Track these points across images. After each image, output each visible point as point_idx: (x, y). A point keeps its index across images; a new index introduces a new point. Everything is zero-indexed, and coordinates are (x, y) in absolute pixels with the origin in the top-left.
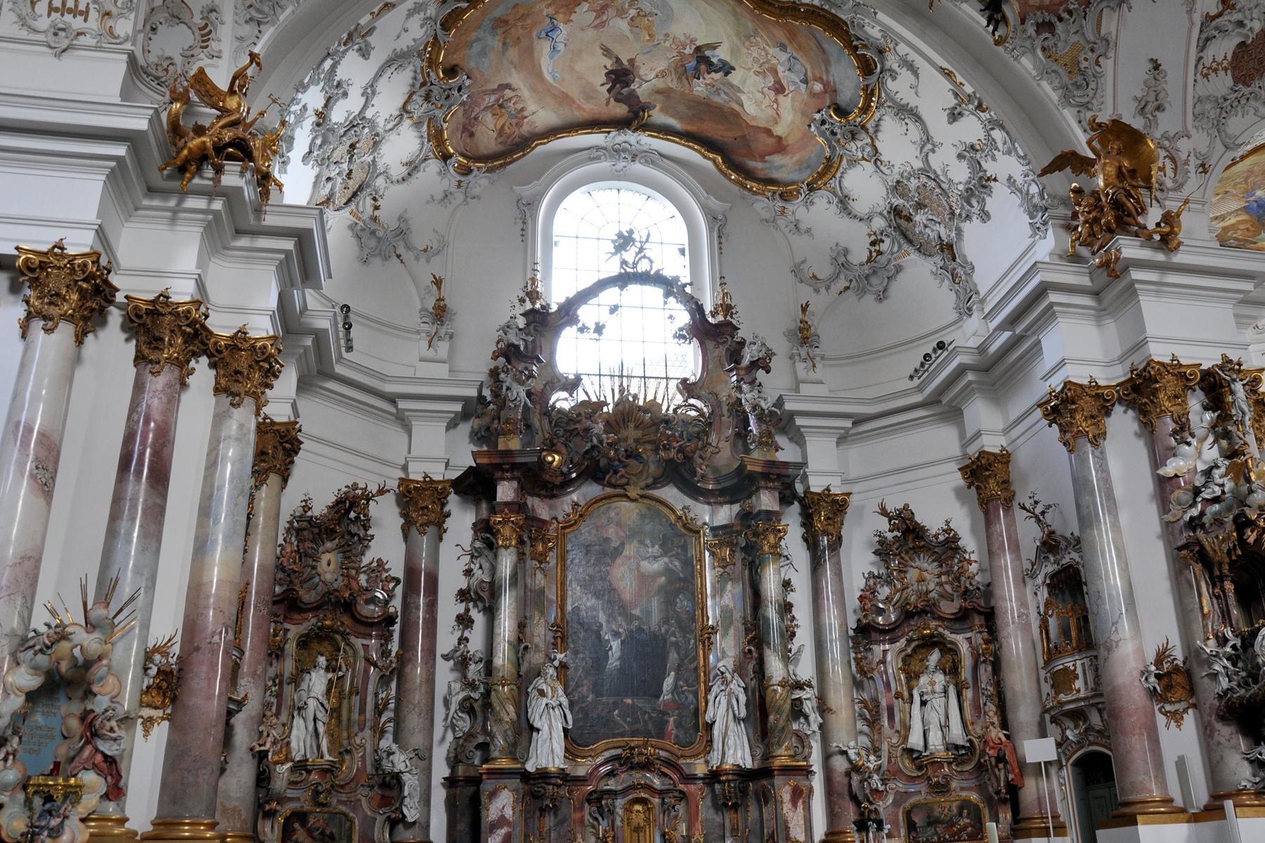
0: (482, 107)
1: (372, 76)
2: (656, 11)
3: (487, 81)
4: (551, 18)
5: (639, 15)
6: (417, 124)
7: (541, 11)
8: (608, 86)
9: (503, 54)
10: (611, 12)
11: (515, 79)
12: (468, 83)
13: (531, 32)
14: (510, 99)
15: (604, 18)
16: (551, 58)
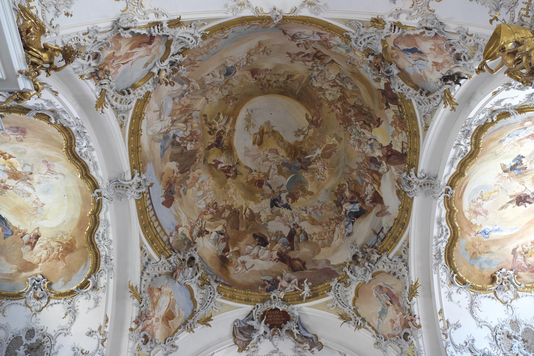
0: (523, 262)
1: (475, 321)
2: (480, 192)
3: (507, 260)
4: (478, 233)
5: (482, 198)
6: (517, 296)
7: (472, 238)
8: (527, 204)
9: (493, 253)
10: (479, 209)
11: (510, 247)
12: (504, 270)
13: (483, 242)
14: (523, 249)
15: (481, 212)
16: (502, 231)
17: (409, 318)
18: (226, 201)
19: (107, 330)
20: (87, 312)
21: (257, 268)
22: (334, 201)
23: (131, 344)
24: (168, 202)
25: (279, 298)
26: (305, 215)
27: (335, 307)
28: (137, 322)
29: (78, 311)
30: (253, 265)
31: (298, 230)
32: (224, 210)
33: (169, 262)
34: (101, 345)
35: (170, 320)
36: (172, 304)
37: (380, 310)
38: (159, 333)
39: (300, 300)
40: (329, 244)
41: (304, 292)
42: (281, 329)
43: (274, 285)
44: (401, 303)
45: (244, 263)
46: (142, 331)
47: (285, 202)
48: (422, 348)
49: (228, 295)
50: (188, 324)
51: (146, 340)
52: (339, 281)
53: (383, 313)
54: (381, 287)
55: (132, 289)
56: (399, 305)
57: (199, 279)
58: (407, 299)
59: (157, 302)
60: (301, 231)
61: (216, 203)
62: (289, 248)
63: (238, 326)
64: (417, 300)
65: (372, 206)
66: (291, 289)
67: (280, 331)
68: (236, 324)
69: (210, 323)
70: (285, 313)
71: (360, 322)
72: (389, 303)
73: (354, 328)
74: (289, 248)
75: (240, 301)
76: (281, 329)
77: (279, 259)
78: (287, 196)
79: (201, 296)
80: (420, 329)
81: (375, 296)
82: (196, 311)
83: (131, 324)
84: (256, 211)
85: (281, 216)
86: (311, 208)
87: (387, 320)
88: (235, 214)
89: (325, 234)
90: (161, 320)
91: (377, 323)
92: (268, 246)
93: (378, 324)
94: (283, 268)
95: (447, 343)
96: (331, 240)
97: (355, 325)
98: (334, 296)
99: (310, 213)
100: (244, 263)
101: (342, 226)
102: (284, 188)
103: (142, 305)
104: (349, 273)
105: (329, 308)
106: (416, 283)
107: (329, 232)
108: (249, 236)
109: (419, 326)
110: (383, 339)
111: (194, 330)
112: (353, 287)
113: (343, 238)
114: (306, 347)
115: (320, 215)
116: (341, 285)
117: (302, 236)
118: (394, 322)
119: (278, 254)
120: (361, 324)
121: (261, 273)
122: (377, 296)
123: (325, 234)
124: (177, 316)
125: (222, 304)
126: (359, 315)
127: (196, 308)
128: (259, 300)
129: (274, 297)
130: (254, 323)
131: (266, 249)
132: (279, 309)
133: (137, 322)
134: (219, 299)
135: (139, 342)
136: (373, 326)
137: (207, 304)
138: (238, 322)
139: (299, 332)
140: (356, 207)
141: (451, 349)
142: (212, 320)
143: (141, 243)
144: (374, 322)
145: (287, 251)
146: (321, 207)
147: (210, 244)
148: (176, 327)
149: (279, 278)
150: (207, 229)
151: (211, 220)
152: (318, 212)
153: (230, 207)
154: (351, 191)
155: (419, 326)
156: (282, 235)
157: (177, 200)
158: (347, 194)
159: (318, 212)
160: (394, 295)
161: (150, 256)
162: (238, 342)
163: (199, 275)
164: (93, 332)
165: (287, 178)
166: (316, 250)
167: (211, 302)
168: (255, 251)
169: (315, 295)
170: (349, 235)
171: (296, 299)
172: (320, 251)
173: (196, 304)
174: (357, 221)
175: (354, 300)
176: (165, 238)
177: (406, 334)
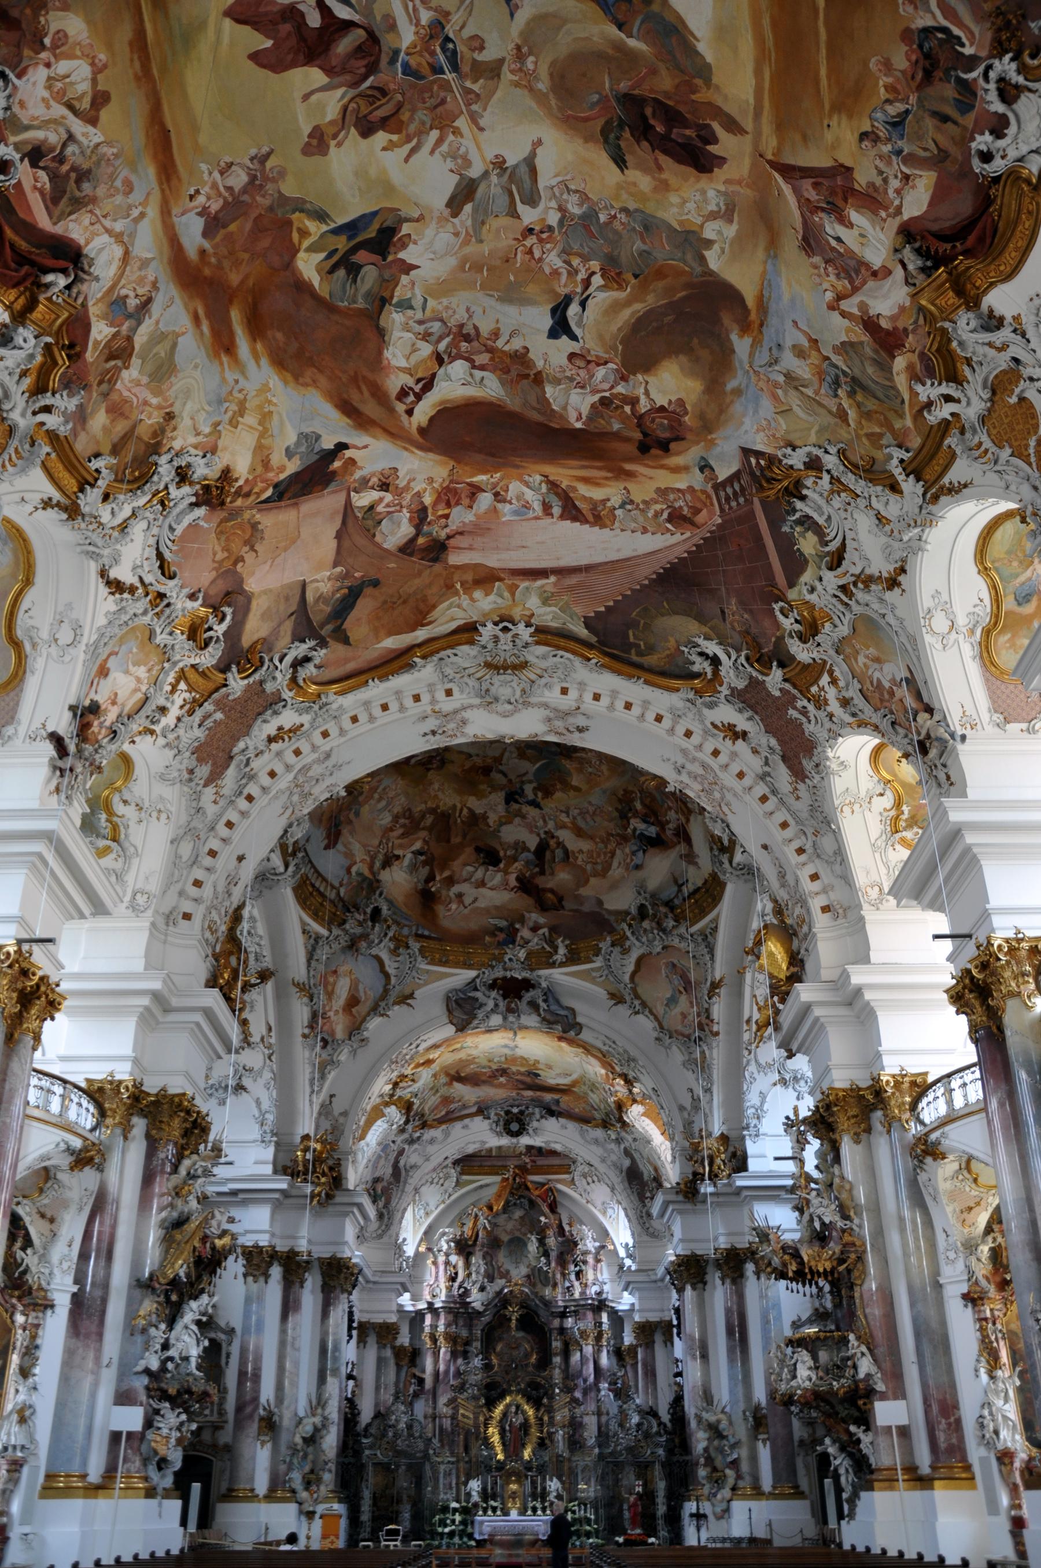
17: (704, 1021)
18: (426, 803)
21: (481, 904)
22: (617, 809)
23: (307, 1054)
24: (333, 838)
26: (566, 820)
30: (476, 900)
31: (552, 842)
32: (423, 817)
33: (344, 930)
36: (355, 985)
37: (668, 996)
38: (340, 1033)
39: (553, 965)
40: (604, 873)
43: (511, 937)
45: (460, 896)
47: (531, 796)
51: (325, 1043)
52: (613, 945)
53: (672, 1001)
54: (674, 965)
55: (297, 985)
57: (391, 940)
60: (559, 844)
61: (409, 810)
62: (537, 869)
65: (675, 840)
74: (537, 869)
75: (457, 965)
76: (520, 998)
77: (519, 888)
78: (535, 789)
79: (396, 965)
84: (479, 811)
85: (524, 817)
86: (577, 811)
87: (677, 1011)
88: (443, 821)
89: (599, 855)
92: (502, 865)
94: (527, 901)
95: (748, 1062)
96: (607, 867)
99: (574, 818)
100: (460, 896)
101: (627, 850)
102: (530, 777)
104: (629, 934)
105: (594, 978)
106: (721, 981)
107: (605, 854)
108: (469, 851)
109: (717, 1034)
112: (634, 955)
113: (627, 869)
115: (592, 823)
116: (618, 949)
117: (559, 853)
119: (518, 879)
121: (487, 911)
123: (599, 855)
125: (428, 971)
126: (637, 996)
131: (499, 871)
133: (311, 1026)
134: (424, 966)
135: (318, 1049)
140: (652, 831)
141: (752, 1068)
143: (303, 924)
145: (533, 876)
146: (594, 813)
147: (403, 874)
149: (517, 926)
150: (396, 852)
151: (403, 836)
152: (589, 819)
153: (433, 811)
154: (642, 803)
155: (717, 1034)
156: (526, 849)
157: (345, 831)
158: (638, 806)
159: (589, 819)
161: (316, 933)
163: (391, 934)
165: (534, 764)
166: (583, 880)
168: (479, 874)
169: (573, 958)
170: (638, 867)
172: (587, 881)
174: (651, 851)
176: (331, 895)
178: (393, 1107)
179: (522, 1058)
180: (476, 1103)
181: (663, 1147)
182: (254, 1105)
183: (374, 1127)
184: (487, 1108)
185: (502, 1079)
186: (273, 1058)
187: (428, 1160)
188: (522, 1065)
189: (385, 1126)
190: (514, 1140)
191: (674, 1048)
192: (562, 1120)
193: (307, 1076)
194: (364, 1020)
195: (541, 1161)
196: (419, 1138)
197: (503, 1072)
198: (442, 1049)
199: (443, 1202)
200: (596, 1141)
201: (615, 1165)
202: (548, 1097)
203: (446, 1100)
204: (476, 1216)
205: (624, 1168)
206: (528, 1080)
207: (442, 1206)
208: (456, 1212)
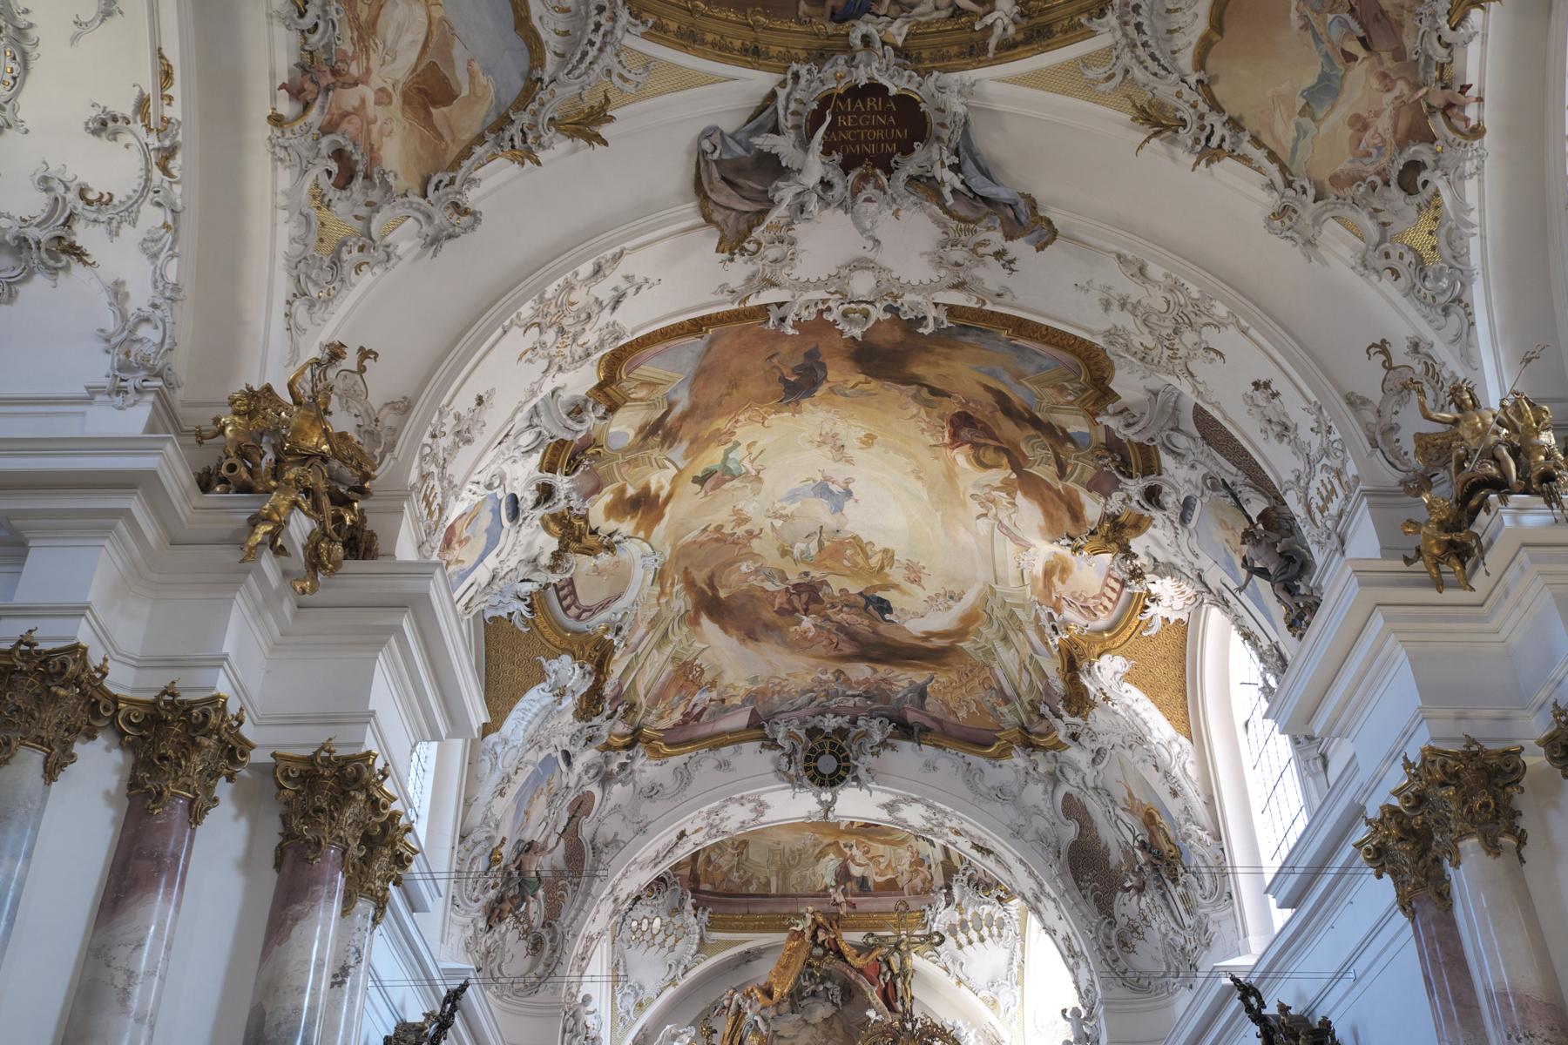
19: (174, 112)
20: (75, 38)
23: (285, 178)
25: (884, 43)
27: (1118, 78)
28: (295, 92)
29: (32, 33)
34: (157, 174)
35: (435, 104)
36: (438, 40)
37: (1310, 80)
39: (975, 52)
41: (995, 15)
42: (889, 171)
44: (1410, 43)
46: (325, 130)
48: (1474, 217)
49: (673, 26)
50: (514, 130)
53: (1325, 89)
56: (1399, 54)
58: (1443, 22)
59: (373, 23)
63: (716, 155)
64: (1485, 26)
66: (937, 9)
67: (884, 179)
68: (707, 145)
69: (605, 131)
70: (907, 107)
71: (1220, 131)
72: (1354, 47)
73: (1194, 159)
75: (722, 51)
76: (889, 171)
80: (1476, 144)
81: (1295, 20)
82: (540, 80)
83: (274, 98)
87: (1336, 119)
90: (397, 100)
91: (1293, 133)
93: (1297, 140)
97: (1198, 148)
98: (1119, 34)
103: (308, 21)
105: (1093, 83)
109: (1477, 132)
110: (1311, 192)
111: (541, 155)
114: (984, 243)
118: (1365, 127)
120: (1223, 140)
122: (1307, 26)
124: (465, 92)
125: (648, 63)
126: (1216, 107)
127: (542, 66)
128: (802, 54)
129: (866, 40)
130: (783, 146)
132: (886, 89)
136: (1272, 146)
137: (585, 54)
138: (716, 138)
139: (963, 182)
142: (612, 119)
144: (1279, 127)
148: (466, 137)
160: (1382, 11)
162: (717, 216)
164: (115, 119)
167: (601, 50)
171: (954, 50)
173: (543, 53)
175: (1205, 47)
177: (1415, 166)
178: (566, 659)
179: (857, 542)
180: (750, 698)
181: (1176, 749)
182: (105, 299)
183: (520, 705)
184: (771, 717)
185: (807, 623)
186: (175, 165)
187: (643, 830)
188: (855, 572)
189: (548, 699)
190: (826, 796)
191: (1331, 228)
192: (928, 750)
193: (283, 244)
194: (467, 153)
195: (866, 904)
196: (623, 766)
197: (809, 594)
198: (678, 451)
199: (673, 982)
200: (1000, 794)
201: (1041, 839)
202: (903, 679)
203: (686, 675)
204: (739, 1013)
205: (1064, 848)
206: (861, 623)
207: (671, 991)
208: (700, 1007)
